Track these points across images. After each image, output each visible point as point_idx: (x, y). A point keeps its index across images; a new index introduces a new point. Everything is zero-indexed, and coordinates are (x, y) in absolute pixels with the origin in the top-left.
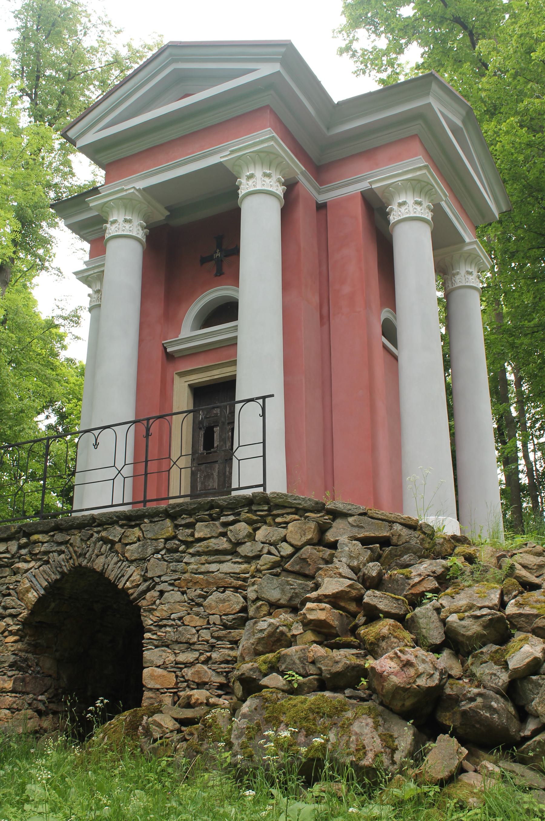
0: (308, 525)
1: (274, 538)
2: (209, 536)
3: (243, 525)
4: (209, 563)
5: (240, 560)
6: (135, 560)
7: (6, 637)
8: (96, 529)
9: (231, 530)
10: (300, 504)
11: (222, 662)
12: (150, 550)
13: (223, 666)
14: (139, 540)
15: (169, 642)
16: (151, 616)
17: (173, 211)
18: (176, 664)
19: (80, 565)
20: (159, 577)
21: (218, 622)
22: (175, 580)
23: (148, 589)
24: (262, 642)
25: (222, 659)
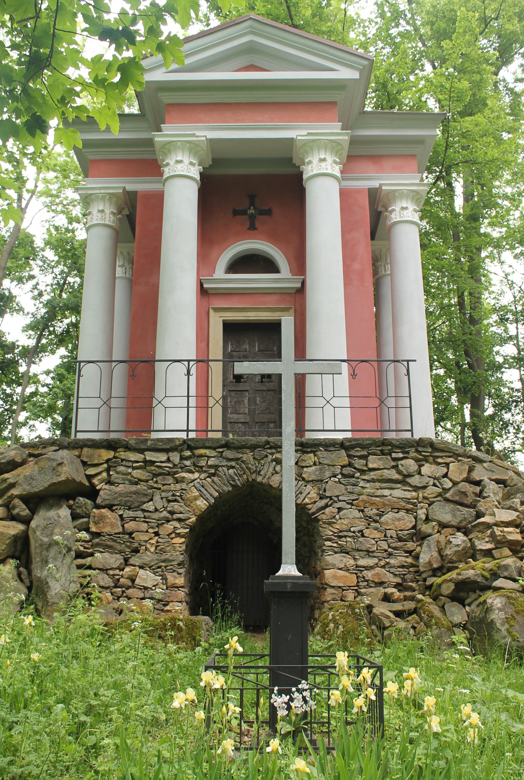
0: (464, 467)
1: (438, 474)
2: (382, 467)
3: (412, 462)
4: (381, 489)
5: (410, 489)
6: (312, 481)
7: (172, 539)
8: (269, 451)
9: (401, 465)
10: (457, 450)
11: (399, 567)
12: (328, 474)
13: (399, 569)
14: (315, 464)
15: (350, 550)
16: (330, 528)
17: (216, 162)
18: (357, 567)
19: (254, 480)
20: (337, 496)
21: (395, 536)
22: (353, 500)
23: (326, 506)
24: (457, 554)
25: (399, 564)
